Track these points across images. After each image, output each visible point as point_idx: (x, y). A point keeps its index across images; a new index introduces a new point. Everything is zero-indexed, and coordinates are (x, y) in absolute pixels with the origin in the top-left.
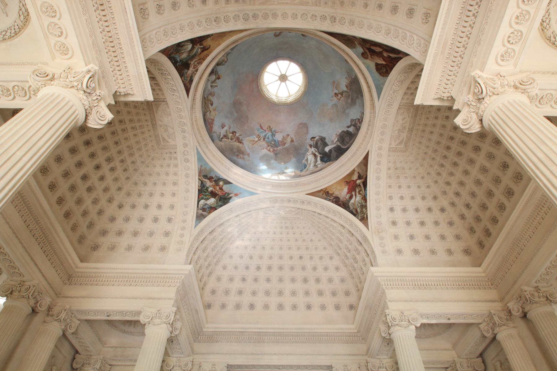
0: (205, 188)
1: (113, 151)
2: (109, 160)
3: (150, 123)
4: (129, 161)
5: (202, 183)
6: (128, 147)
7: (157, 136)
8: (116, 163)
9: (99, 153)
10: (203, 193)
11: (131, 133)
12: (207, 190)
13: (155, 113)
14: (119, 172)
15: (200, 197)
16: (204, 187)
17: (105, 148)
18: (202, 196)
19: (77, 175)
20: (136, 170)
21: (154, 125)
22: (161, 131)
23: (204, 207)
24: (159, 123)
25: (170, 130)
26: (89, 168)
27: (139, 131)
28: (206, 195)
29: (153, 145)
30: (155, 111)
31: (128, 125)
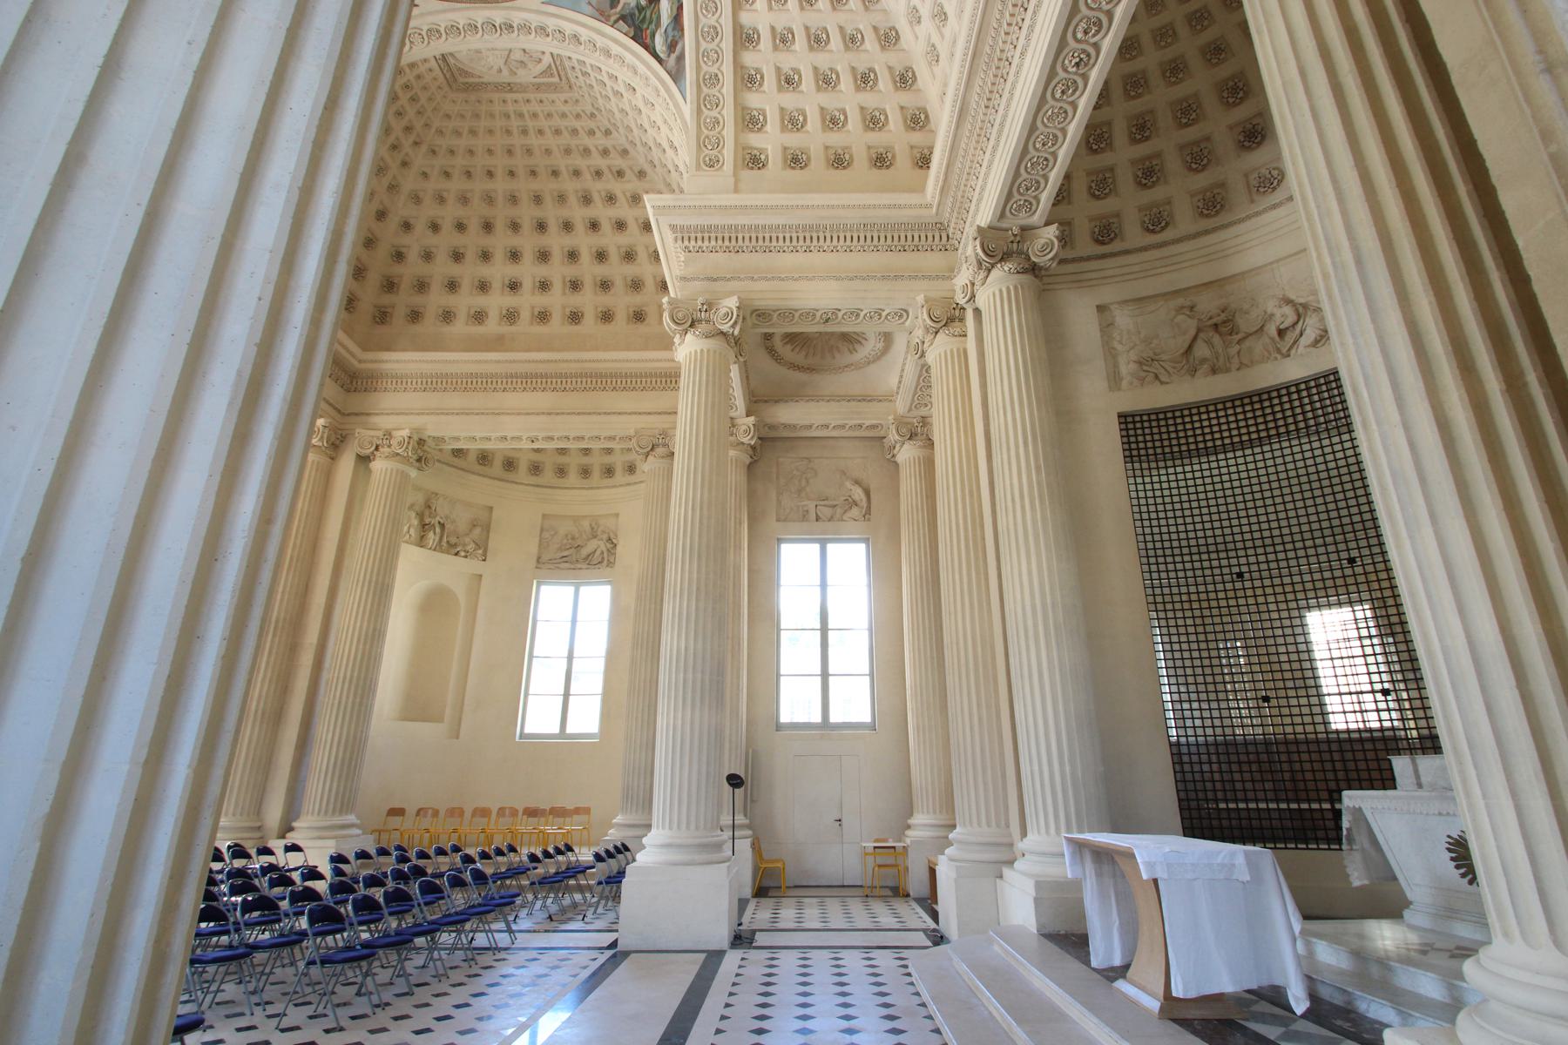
0: (637, 12)
1: (570, 186)
2: (587, 200)
3: (509, 96)
4: (598, 161)
5: (623, 18)
6: (568, 151)
7: (538, 87)
8: (597, 188)
9: (565, 213)
10: (645, 26)
11: (533, 140)
12: (643, 9)
13: (481, 80)
14: (617, 187)
15: (648, 41)
16: (634, 14)
17: (561, 198)
18: (648, 31)
19: (588, 269)
20: (625, 152)
21: (510, 87)
22: (525, 76)
23: (669, 40)
24: (505, 77)
25: (517, 56)
26: (584, 242)
27: (530, 124)
28: (651, 22)
29: (563, 99)
30: (477, 80)
31: (517, 141)
